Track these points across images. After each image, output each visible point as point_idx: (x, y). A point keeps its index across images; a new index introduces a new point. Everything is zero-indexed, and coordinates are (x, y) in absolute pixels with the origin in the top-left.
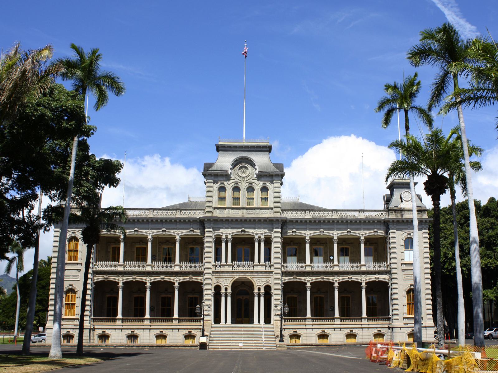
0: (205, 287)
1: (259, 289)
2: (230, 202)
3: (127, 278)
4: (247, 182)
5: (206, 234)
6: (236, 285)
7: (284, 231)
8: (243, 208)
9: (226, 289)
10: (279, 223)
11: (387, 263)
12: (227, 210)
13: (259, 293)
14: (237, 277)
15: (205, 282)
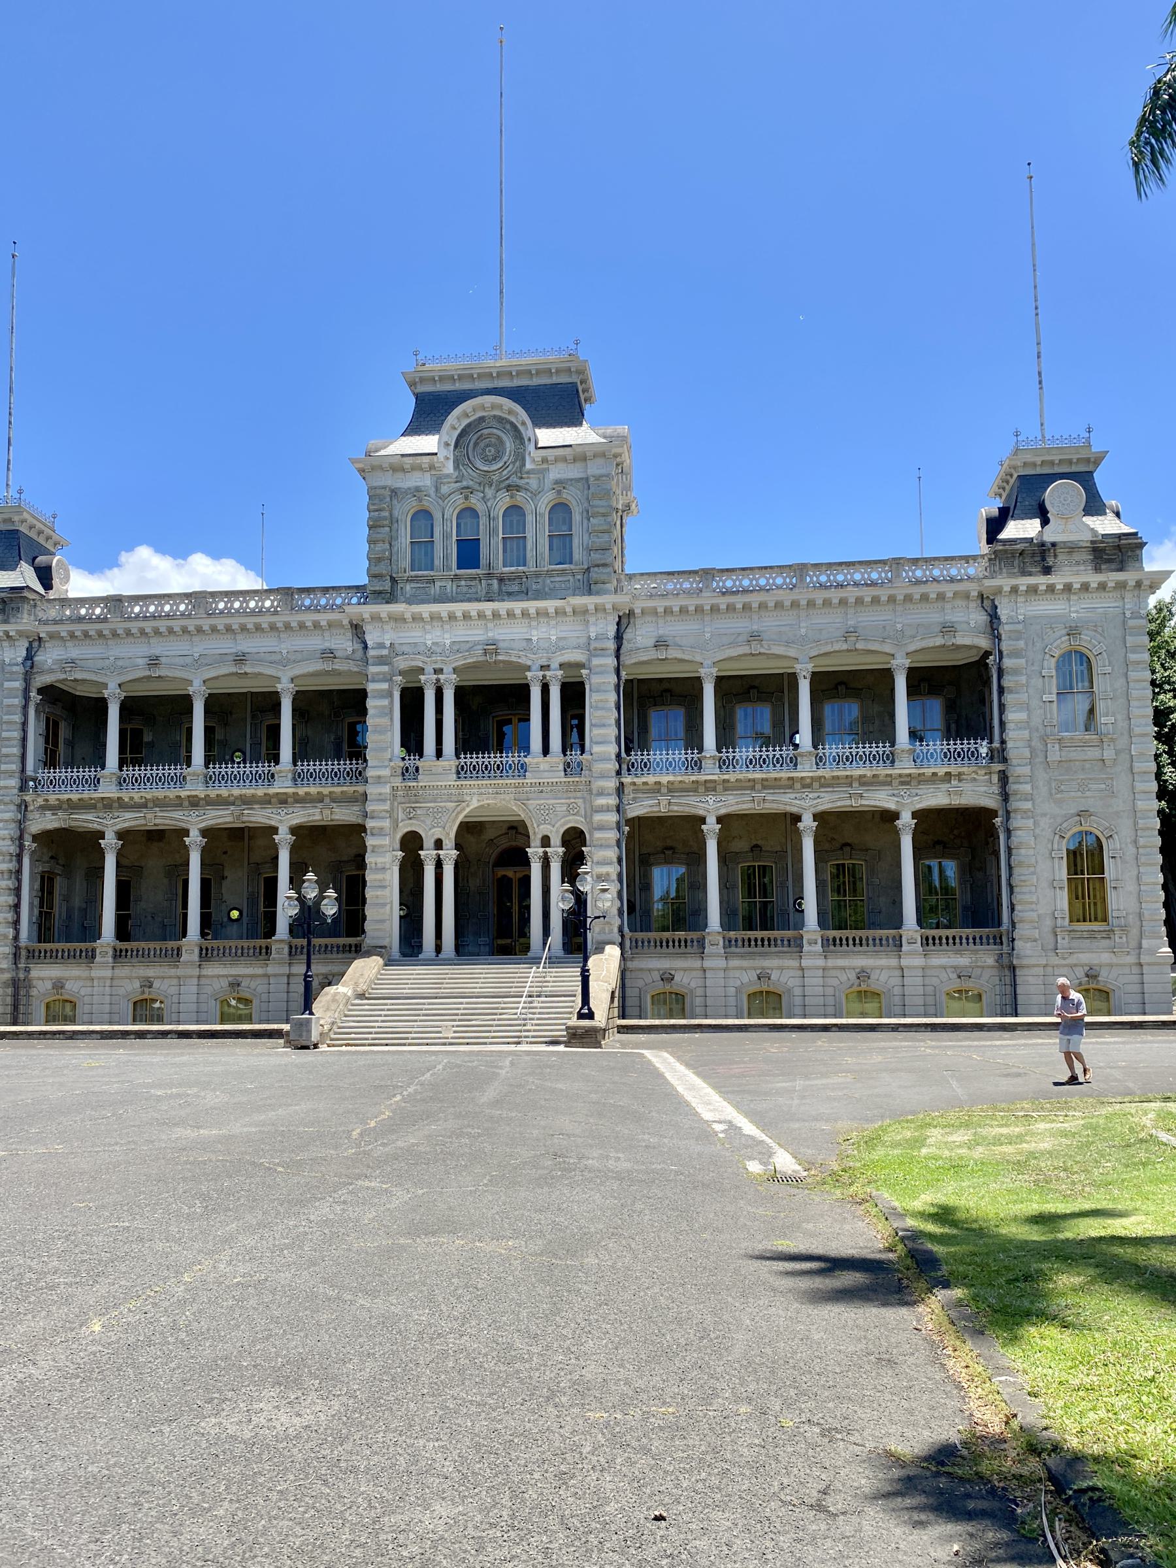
0: (370, 841)
1: (546, 841)
2: (446, 557)
3: (128, 820)
4: (503, 485)
5: (373, 669)
6: (469, 830)
7: (626, 646)
8: (489, 576)
9: (439, 844)
10: (610, 618)
11: (991, 742)
12: (438, 584)
13: (546, 853)
14: (475, 804)
15: (370, 824)
